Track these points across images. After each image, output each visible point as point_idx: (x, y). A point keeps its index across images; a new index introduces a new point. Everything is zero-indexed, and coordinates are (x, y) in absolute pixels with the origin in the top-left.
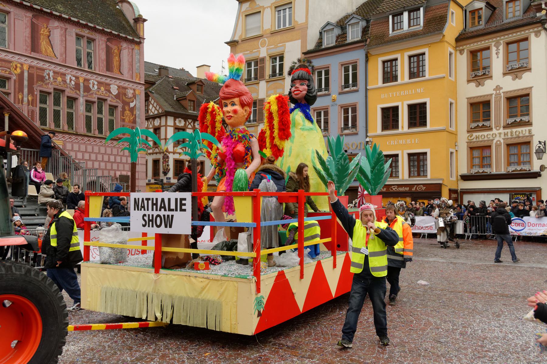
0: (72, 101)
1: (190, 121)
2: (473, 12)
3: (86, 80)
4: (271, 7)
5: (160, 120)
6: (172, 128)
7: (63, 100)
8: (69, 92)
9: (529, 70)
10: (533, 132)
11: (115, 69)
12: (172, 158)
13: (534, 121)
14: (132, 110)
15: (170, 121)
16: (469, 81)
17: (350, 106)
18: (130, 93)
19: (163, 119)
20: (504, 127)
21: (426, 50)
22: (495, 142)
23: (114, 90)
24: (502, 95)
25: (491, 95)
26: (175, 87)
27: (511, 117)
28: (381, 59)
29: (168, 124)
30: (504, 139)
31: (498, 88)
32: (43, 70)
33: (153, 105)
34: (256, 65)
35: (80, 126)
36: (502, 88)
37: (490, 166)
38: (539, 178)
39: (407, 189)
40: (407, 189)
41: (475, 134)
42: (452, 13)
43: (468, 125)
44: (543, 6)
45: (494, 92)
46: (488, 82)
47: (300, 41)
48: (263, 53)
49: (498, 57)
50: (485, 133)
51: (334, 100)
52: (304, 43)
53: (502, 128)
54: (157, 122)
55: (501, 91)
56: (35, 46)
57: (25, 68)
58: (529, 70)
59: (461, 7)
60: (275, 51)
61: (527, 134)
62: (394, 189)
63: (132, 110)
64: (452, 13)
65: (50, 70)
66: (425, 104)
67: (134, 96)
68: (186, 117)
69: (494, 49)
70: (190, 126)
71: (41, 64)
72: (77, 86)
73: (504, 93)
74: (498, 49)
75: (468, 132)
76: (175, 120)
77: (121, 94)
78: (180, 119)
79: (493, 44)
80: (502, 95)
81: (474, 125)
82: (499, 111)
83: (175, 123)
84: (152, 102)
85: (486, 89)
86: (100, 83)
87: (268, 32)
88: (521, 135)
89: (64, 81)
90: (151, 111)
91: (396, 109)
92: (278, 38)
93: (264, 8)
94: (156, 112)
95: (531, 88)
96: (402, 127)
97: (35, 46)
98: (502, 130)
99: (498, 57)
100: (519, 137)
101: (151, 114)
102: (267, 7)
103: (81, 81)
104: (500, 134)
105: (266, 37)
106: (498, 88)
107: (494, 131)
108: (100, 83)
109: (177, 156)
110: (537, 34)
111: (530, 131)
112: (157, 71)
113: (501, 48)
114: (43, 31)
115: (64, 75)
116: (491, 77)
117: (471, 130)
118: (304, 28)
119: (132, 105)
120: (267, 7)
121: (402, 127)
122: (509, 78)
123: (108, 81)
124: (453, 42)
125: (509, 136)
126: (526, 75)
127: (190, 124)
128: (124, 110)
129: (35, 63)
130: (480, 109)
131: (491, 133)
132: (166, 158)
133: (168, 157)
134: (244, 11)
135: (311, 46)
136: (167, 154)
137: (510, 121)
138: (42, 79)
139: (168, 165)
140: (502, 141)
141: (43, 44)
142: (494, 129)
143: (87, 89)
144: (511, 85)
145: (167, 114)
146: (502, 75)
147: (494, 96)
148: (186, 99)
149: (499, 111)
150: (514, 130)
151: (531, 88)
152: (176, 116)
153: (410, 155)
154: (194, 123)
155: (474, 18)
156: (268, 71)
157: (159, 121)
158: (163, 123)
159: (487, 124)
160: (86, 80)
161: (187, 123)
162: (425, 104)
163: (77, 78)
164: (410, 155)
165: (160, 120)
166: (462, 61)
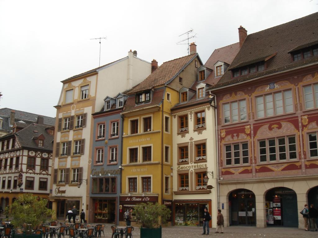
1: (39, 152)
2: (183, 94)
4: (78, 87)
5: (20, 152)
6: (27, 157)
9: (205, 129)
10: (208, 166)
12: (24, 175)
13: (208, 160)
15: (26, 153)
16: (178, 134)
17: (114, 147)
19: (21, 151)
20: (195, 163)
21: (152, 115)
22: (190, 171)
24: (193, 143)
25: (189, 142)
26: (35, 131)
27: (198, 156)
28: (130, 119)
29: (24, 155)
30: (194, 169)
31: (191, 139)
33: (17, 142)
34: (82, 118)
36: (193, 139)
37: (188, 186)
38: (210, 193)
39: (140, 199)
40: (140, 199)
41: (181, 166)
42: (168, 95)
43: (178, 160)
44: (210, 93)
45: (190, 141)
46: (187, 135)
47: (92, 107)
48: (73, 113)
49: (191, 121)
50: (186, 166)
51: (106, 144)
52: (93, 109)
53: (193, 163)
54: (18, 153)
55: (193, 140)
58: (205, 129)
59: (177, 91)
60: (79, 113)
61: (205, 167)
62: (134, 199)
64: (168, 95)
66: (150, 147)
68: (36, 150)
69: (189, 116)
70: (39, 156)
73: (194, 141)
74: (191, 116)
75: (178, 164)
76: (28, 152)
78: (32, 151)
79: (189, 113)
80: (193, 143)
81: (181, 160)
82: (192, 152)
83: (28, 154)
84: (17, 141)
85: (186, 139)
87: (76, 101)
88: (202, 167)
90: (16, 146)
91: (136, 149)
92: (81, 104)
93: (75, 87)
94: (18, 147)
95: (206, 139)
96: (139, 161)
98: (193, 164)
99: (191, 121)
100: (201, 169)
101: (16, 148)
102: (77, 87)
104: (192, 166)
105: (75, 104)
106: (191, 139)
107: (190, 165)
109: (28, 175)
110: (209, 109)
111: (206, 165)
112: (37, 119)
113: (193, 115)
116: (188, 132)
117: (179, 164)
118: (94, 99)
120: (77, 87)
121: (139, 161)
122: (196, 133)
124: (169, 112)
125: (197, 168)
126: (204, 132)
127: (39, 154)
130: (183, 150)
131: (188, 165)
132: (21, 176)
133: (22, 176)
134: (66, 89)
135: (98, 110)
136: (22, 173)
137: (198, 158)
139: (22, 181)
140: (193, 171)
142: (190, 163)
145: (23, 148)
146: (193, 131)
147: (189, 143)
148: (38, 139)
149: (192, 152)
150: (199, 164)
151: (206, 139)
152: (29, 149)
153: (143, 178)
154: (42, 154)
155: (183, 97)
156: (76, 124)
157: (19, 153)
158: (21, 154)
159: (186, 160)
161: (37, 154)
162: (150, 147)
164: (143, 178)
165: (20, 152)
166: (175, 122)
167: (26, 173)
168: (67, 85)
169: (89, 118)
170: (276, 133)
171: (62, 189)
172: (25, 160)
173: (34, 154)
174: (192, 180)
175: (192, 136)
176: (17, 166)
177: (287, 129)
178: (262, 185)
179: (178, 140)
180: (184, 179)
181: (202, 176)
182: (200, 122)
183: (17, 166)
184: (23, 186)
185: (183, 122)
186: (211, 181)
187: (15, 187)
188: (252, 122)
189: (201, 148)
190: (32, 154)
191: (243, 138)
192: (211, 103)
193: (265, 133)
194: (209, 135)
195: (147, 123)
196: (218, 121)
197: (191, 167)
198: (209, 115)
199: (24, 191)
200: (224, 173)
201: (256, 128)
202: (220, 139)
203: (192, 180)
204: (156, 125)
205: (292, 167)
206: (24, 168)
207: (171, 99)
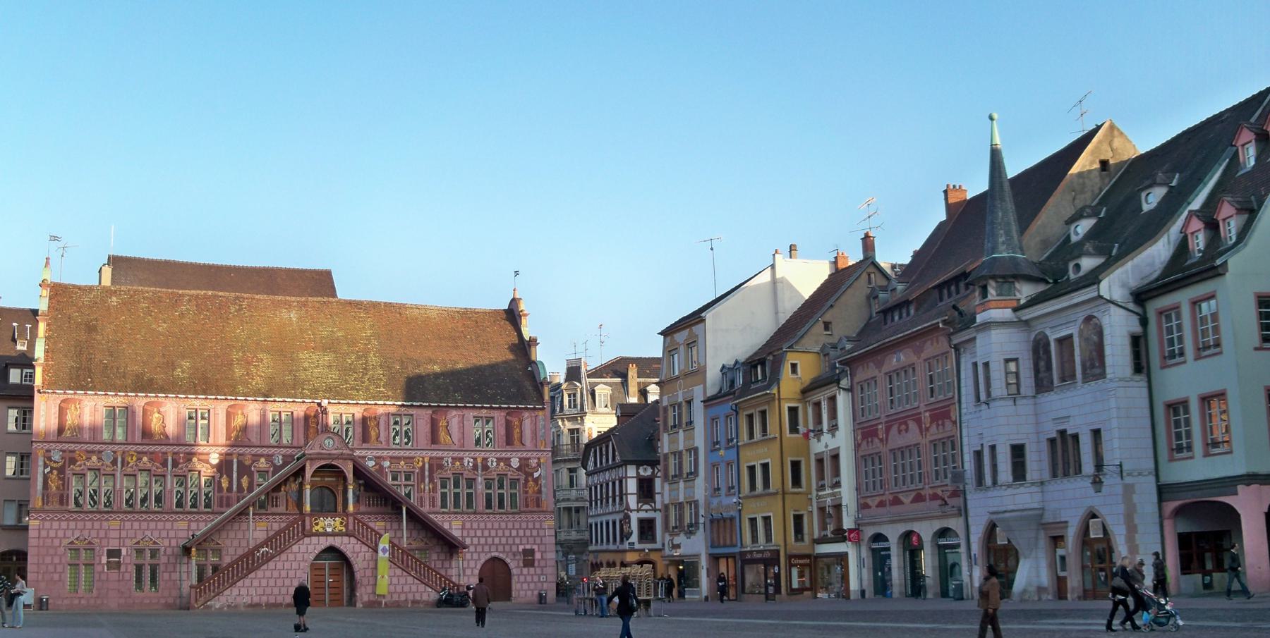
0: (471, 483)
3: (485, 460)
7: (463, 483)
8: (467, 475)
11: (516, 442)
12: (634, 517)
13: (843, 483)
14: (536, 480)
15: (631, 471)
18: (534, 463)
21: (766, 407)
23: (515, 463)
32: (442, 458)
35: (480, 503)
42: (794, 366)
54: (621, 472)
56: (434, 439)
57: (426, 460)
63: (536, 480)
64: (794, 366)
65: (448, 457)
67: (539, 465)
71: (440, 454)
72: (475, 467)
77: (524, 463)
86: (499, 460)
89: (462, 464)
97: (434, 439)
103: (479, 461)
108: (499, 460)
109: (643, 515)
114: (442, 423)
115: (461, 459)
119: (536, 475)
123: (509, 455)
124: (799, 397)
128: (527, 481)
129: (435, 454)
132: (627, 517)
135: (711, 392)
138: (441, 467)
141: (442, 434)
143: (485, 468)
145: (625, 463)
152: (638, 464)
160: (485, 460)
163: (475, 459)
167: (638, 510)
168: (669, 339)
169: (698, 407)
171: (677, 540)
172: (632, 486)
173: (649, 472)
176: (621, 499)
178: (895, 526)
183: (621, 499)
184: (634, 538)
187: (622, 541)
188: (883, 420)
190: (646, 472)
192: (838, 382)
193: (897, 440)
194: (842, 440)
199: (637, 546)
200: (863, 506)
206: (632, 501)
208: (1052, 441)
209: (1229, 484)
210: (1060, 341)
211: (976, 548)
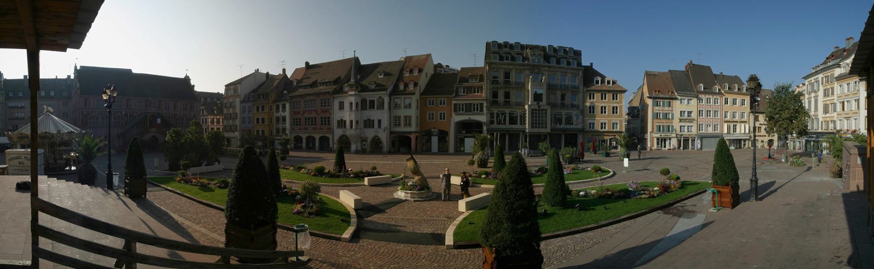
82: (281, 119)
85: (278, 115)
130: (278, 119)
144: (283, 114)
149: (281, 119)
166: (275, 107)
170: (310, 116)
174: (281, 131)
175: (281, 114)
177: (314, 115)
179: (276, 115)
180: (278, 130)
181: (284, 129)
182: (284, 107)
185: (278, 108)
186: (288, 132)
189: (284, 119)
191: (299, 116)
193: (307, 115)
194: (287, 114)
195: (263, 109)
196: (291, 108)
197: (281, 126)
198: (287, 105)
201: (304, 112)
202: (291, 116)
203: (281, 131)
204: (266, 110)
205: (315, 129)
207: (273, 97)
208: (365, 121)
209: (410, 133)
210: (370, 101)
211: (335, 141)
